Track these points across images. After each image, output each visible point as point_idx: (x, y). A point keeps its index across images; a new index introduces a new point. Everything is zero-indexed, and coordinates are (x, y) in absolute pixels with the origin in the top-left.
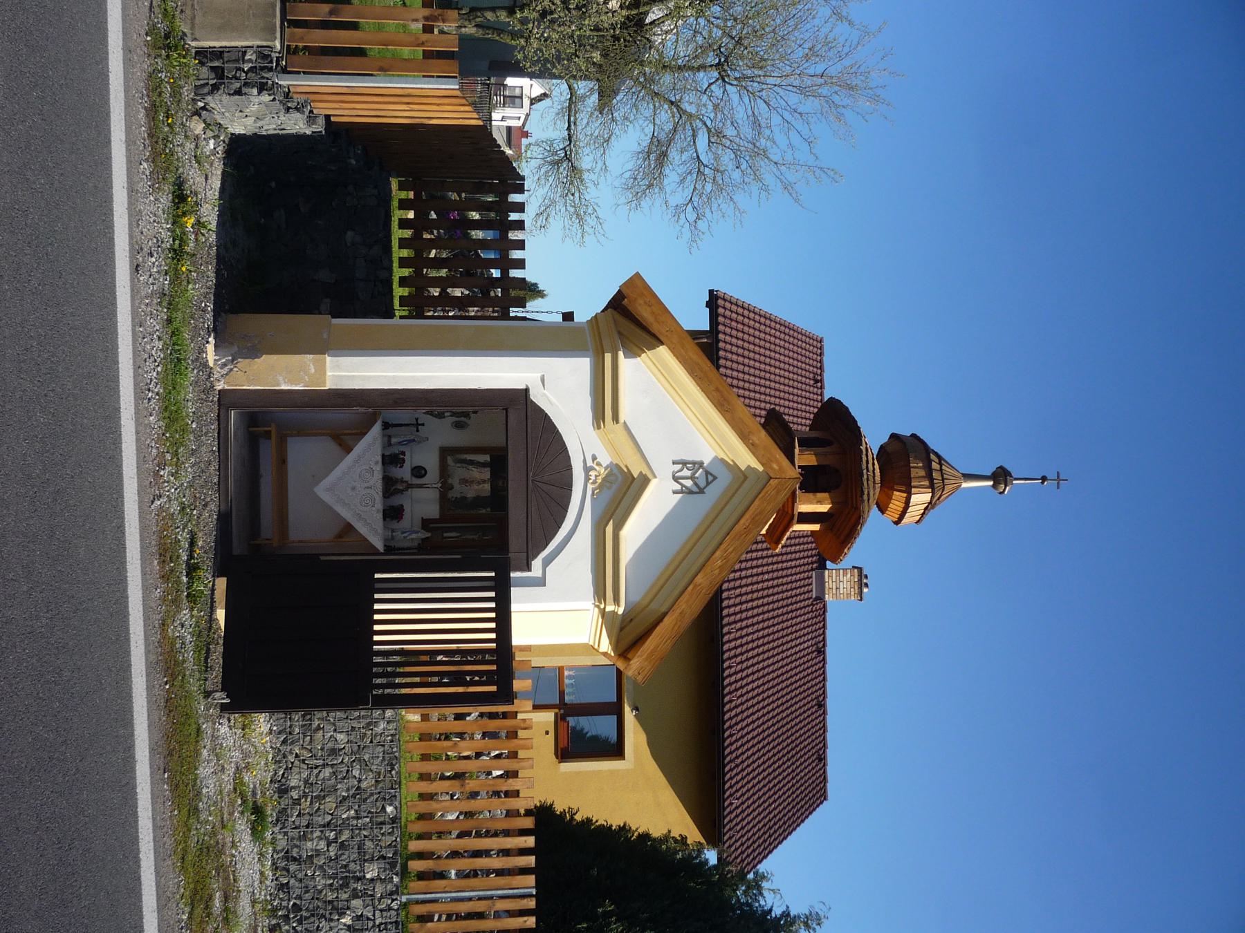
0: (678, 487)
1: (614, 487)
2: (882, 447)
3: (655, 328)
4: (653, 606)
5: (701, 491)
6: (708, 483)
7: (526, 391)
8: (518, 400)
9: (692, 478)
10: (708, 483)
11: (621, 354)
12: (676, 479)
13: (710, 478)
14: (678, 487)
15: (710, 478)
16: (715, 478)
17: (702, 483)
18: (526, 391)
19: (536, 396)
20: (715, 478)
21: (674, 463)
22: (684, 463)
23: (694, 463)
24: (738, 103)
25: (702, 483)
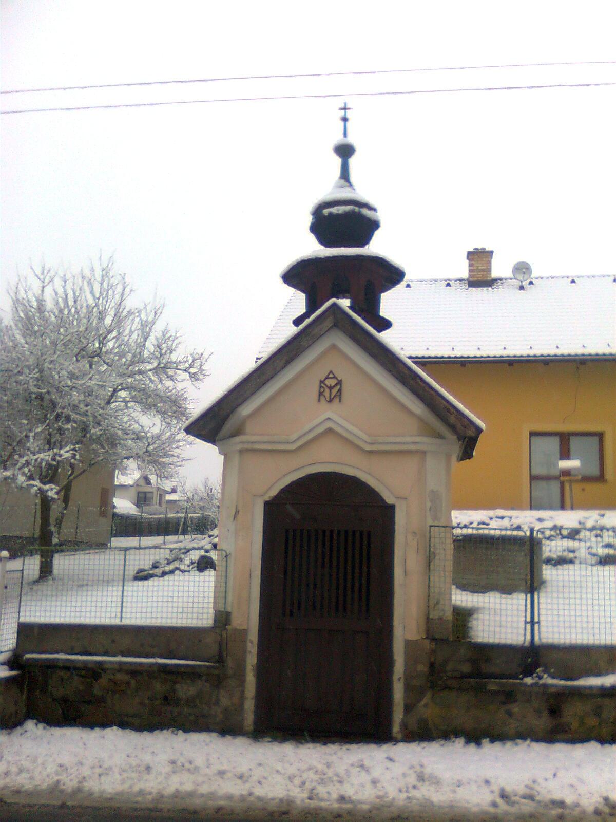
0: (337, 399)
5: (340, 383)
6: (334, 377)
10: (334, 377)
12: (330, 401)
13: (331, 375)
15: (331, 375)
16: (331, 372)
20: (331, 372)
21: (319, 400)
22: (321, 394)
23: (321, 387)
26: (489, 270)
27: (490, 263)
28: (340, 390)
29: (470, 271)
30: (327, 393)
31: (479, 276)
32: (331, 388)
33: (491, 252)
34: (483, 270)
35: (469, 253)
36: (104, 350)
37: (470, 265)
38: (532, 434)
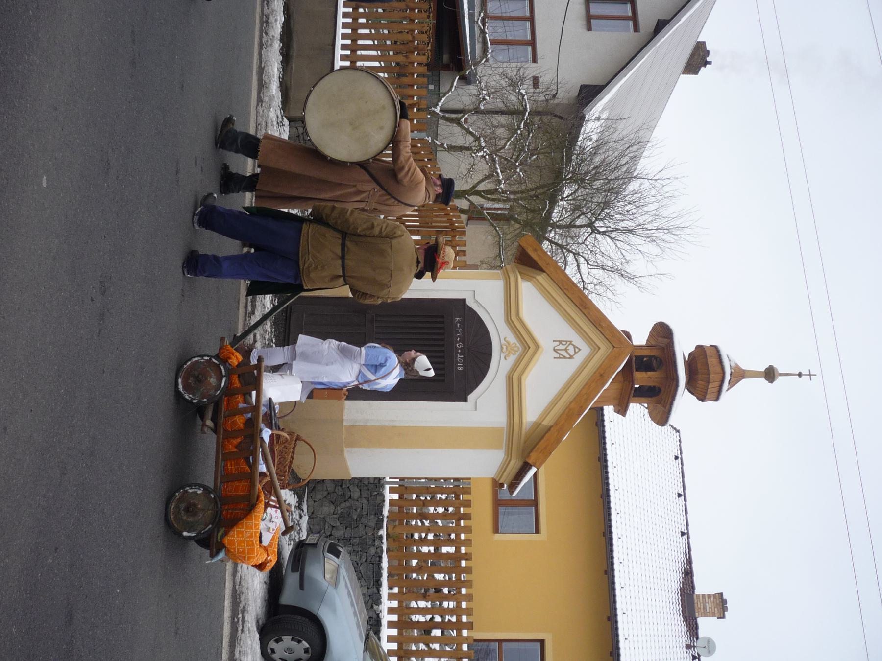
0: (557, 355)
1: (518, 354)
2: (690, 354)
3: (540, 263)
4: (545, 423)
5: (571, 357)
6: (575, 353)
7: (464, 300)
8: (459, 306)
9: (566, 350)
10: (575, 353)
11: (519, 277)
12: (555, 350)
14: (557, 355)
16: (580, 350)
17: (572, 353)
18: (464, 300)
19: (470, 303)
20: (580, 350)
22: (560, 342)
24: (605, 244)
25: (572, 353)
26: (705, 615)
27: (713, 615)
28: (565, 357)
29: (703, 596)
30: (561, 347)
31: (698, 604)
32: (566, 350)
33: (724, 617)
34: (705, 608)
35: (721, 594)
36: (598, 236)
37: (709, 596)
38: (542, 642)
